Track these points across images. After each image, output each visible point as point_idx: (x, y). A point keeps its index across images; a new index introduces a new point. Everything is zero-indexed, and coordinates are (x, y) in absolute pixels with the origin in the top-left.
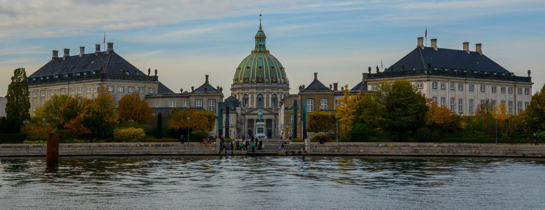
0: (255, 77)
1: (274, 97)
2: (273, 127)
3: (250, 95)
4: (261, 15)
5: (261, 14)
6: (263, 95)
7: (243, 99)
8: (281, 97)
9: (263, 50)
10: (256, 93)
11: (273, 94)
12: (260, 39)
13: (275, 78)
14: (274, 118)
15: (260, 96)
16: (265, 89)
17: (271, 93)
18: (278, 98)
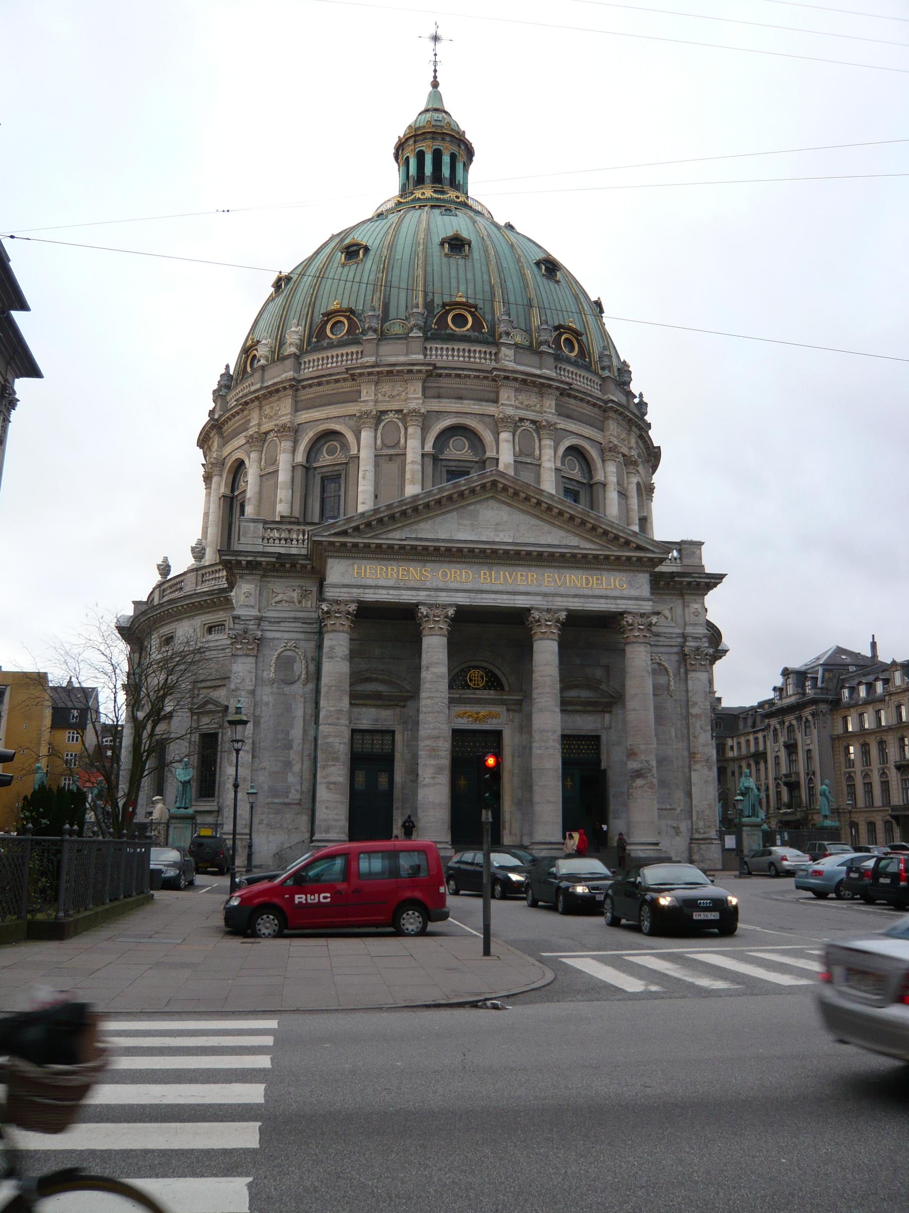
0: (420, 301)
1: (576, 473)
2: (631, 704)
3: (366, 435)
4: (436, 38)
5: (439, 33)
6: (487, 436)
7: (299, 472)
8: (623, 495)
9: (462, 199)
10: (425, 420)
11: (567, 443)
12: (438, 144)
13: (577, 333)
14: (647, 607)
15: (458, 450)
16: (507, 395)
17: (558, 435)
18: (604, 485)
